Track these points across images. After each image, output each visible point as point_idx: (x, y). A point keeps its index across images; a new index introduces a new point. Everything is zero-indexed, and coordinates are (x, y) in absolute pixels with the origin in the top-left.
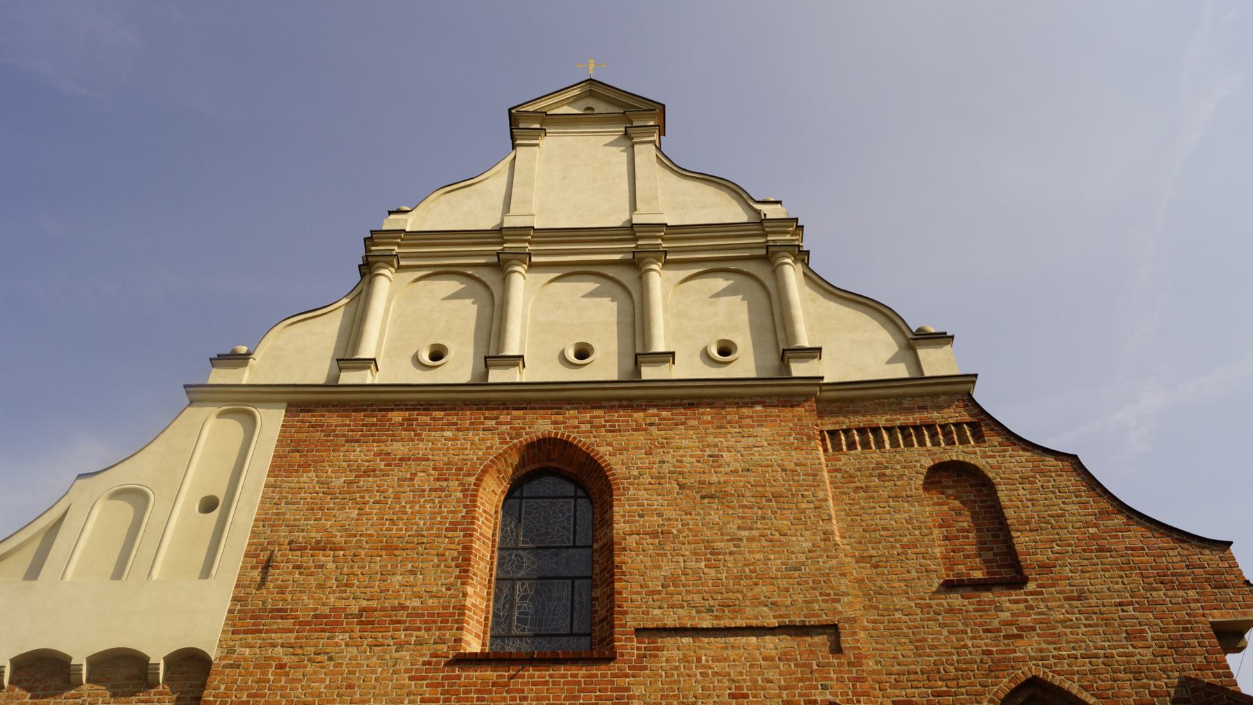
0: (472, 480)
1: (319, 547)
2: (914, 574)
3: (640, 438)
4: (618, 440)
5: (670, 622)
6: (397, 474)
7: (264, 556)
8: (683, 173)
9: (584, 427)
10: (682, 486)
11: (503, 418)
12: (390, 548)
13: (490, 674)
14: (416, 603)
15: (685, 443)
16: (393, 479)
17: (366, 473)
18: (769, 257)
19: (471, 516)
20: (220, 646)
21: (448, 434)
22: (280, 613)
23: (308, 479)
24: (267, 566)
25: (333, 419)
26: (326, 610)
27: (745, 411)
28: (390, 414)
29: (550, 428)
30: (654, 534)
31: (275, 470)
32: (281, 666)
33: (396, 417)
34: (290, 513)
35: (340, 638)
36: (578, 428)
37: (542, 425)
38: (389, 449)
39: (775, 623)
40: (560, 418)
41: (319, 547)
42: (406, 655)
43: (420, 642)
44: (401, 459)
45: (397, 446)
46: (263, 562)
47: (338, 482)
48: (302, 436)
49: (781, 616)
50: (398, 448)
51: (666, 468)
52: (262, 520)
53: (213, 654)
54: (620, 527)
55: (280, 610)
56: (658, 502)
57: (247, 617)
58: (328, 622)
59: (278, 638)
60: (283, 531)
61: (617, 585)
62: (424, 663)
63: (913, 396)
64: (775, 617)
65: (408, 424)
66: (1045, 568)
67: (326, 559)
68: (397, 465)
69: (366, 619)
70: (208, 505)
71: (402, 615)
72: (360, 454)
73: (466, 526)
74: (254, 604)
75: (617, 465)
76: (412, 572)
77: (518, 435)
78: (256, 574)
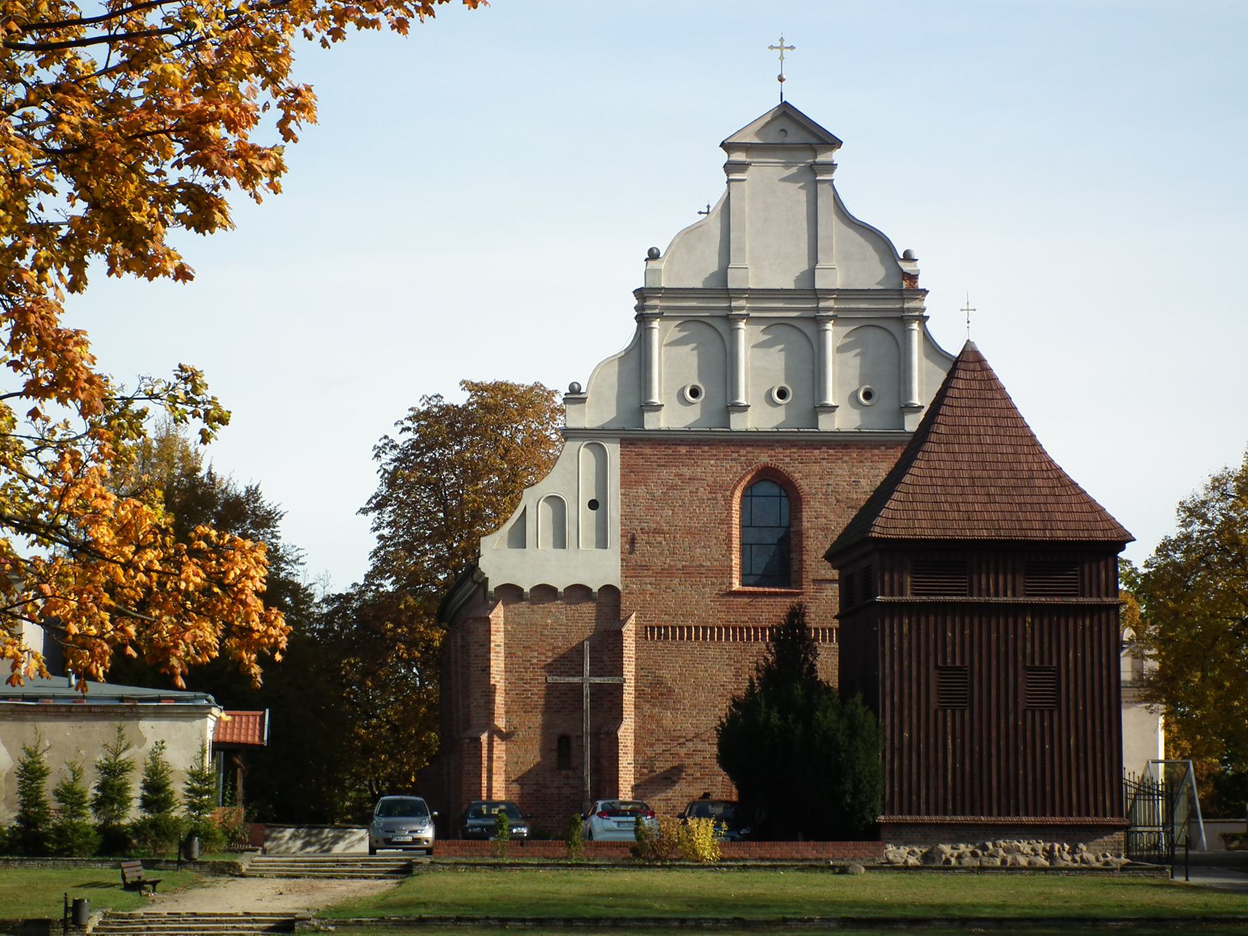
0: (728, 493)
1: (658, 531)
3: (816, 468)
9: (787, 460)
10: (838, 501)
11: (743, 452)
13: (746, 600)
15: (840, 472)
17: (673, 487)
18: (903, 320)
19: (730, 516)
21: (712, 462)
23: (641, 490)
24: (632, 541)
25: (648, 451)
27: (876, 451)
28: (679, 448)
29: (768, 459)
31: (625, 483)
33: (683, 450)
34: (639, 512)
35: (676, 581)
36: (786, 461)
37: (764, 458)
38: (681, 472)
40: (773, 453)
41: (658, 531)
42: (707, 590)
43: (713, 584)
48: (632, 462)
50: (686, 472)
52: (626, 517)
54: (806, 524)
57: (630, 568)
58: (668, 572)
59: (647, 580)
61: (805, 557)
65: (689, 455)
69: (686, 572)
73: (728, 521)
75: (804, 485)
77: (751, 464)
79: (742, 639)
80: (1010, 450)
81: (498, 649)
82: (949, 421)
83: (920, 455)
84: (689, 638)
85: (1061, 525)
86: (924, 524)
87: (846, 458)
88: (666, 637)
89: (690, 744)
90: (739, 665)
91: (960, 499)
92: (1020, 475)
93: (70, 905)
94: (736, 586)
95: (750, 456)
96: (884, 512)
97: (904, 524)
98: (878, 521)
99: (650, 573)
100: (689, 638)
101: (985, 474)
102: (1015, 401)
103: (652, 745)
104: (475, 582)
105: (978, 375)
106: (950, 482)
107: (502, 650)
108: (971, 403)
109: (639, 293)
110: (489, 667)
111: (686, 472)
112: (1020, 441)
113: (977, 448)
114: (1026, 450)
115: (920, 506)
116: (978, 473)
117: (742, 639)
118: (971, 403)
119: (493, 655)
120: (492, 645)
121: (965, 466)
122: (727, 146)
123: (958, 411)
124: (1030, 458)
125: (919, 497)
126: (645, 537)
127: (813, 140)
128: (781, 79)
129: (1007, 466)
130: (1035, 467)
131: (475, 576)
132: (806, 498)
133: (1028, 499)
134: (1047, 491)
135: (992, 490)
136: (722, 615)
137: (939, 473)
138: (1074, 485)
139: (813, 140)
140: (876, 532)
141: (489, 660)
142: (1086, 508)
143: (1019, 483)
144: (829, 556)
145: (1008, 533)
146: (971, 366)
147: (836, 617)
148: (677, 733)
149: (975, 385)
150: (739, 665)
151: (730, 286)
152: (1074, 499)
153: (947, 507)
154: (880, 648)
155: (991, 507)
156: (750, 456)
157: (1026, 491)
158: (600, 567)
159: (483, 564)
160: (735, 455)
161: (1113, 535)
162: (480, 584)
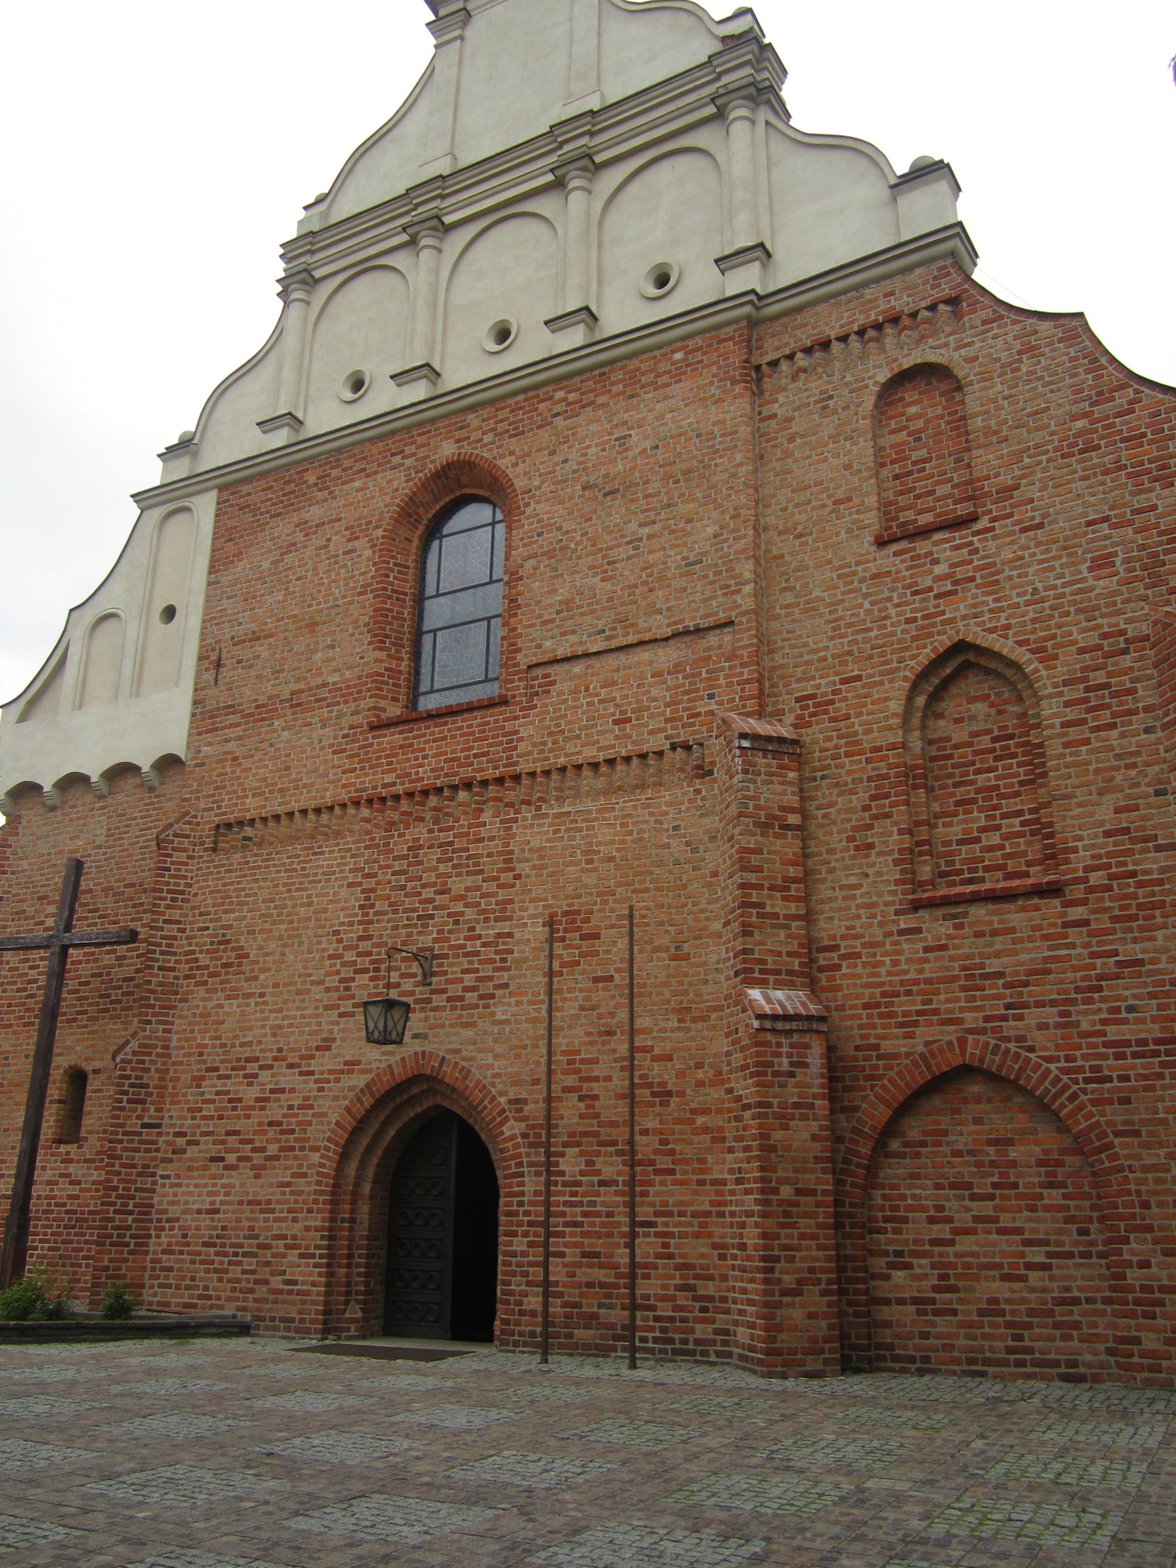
2: (843, 535)
3: (545, 435)
5: (560, 653)
6: (316, 541)
7: (214, 657)
14: (335, 678)
15: (593, 428)
20: (188, 747)
21: (357, 484)
22: (230, 709)
24: (218, 665)
26: (263, 700)
30: (550, 554)
32: (235, 759)
37: (447, 450)
39: (669, 631)
44: (317, 526)
46: (212, 661)
47: (266, 565)
49: (676, 623)
50: (315, 513)
55: (229, 707)
57: (205, 718)
59: (232, 733)
62: (344, 736)
63: (878, 280)
64: (668, 626)
66: (1006, 492)
67: (262, 649)
68: (315, 533)
69: (296, 703)
71: (324, 693)
72: (283, 529)
74: (210, 705)
76: (332, 647)
77: (424, 467)
78: (209, 676)
89: (264, 1076)
90: (370, 883)
99: (236, 718)
103: (198, 1080)
126: (237, 651)
136: (351, 778)
150: (370, 883)
160: (397, 459)
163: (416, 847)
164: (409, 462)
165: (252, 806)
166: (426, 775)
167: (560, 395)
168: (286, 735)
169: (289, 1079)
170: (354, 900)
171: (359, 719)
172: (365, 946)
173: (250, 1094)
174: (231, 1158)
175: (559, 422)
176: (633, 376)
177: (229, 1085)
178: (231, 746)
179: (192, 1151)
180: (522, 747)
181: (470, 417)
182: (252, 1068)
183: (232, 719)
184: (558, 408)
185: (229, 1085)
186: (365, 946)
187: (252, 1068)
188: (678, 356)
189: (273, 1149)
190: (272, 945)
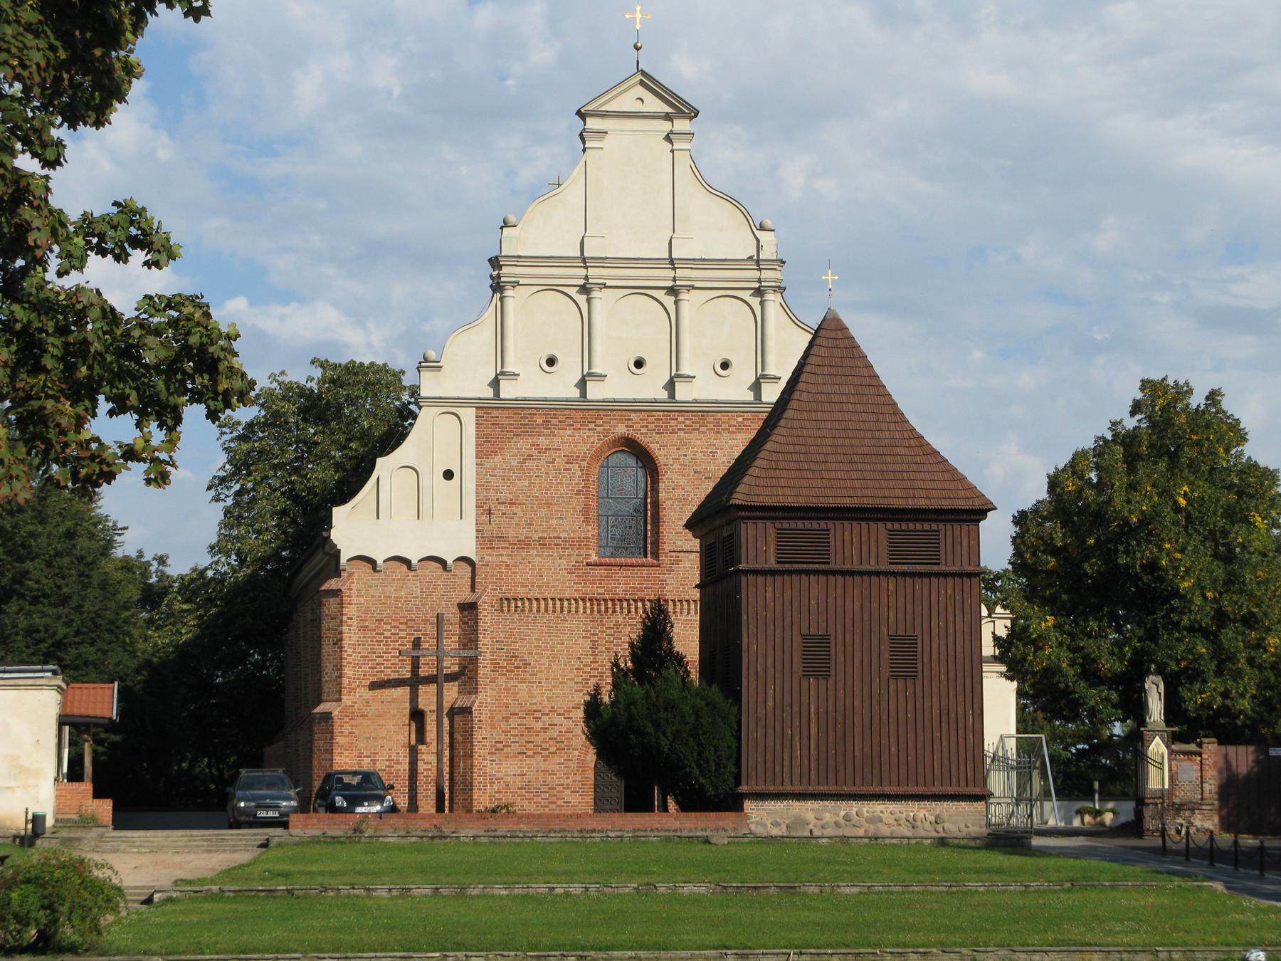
0: (585, 464)
1: (512, 503)
3: (674, 438)
4: (665, 439)
5: (685, 548)
8: (710, 188)
9: (644, 430)
12: (548, 505)
14: (565, 535)
15: (698, 442)
16: (543, 462)
21: (569, 432)
30: (679, 500)
31: (479, 455)
37: (621, 430)
41: (512, 503)
42: (564, 561)
45: (542, 439)
46: (485, 510)
47: (515, 463)
50: (543, 441)
51: (688, 459)
53: (474, 557)
56: (682, 481)
57: (485, 541)
58: (524, 544)
59: (505, 552)
60: (492, 493)
69: (542, 543)
70: (448, 475)
72: (523, 444)
75: (661, 456)
79: (599, 612)
80: (872, 418)
81: (350, 622)
82: (812, 388)
83: (782, 423)
84: (546, 610)
85: (923, 493)
86: (787, 491)
87: (702, 429)
88: (523, 611)
91: (823, 467)
92: (883, 443)
93: (30, 817)
94: (594, 558)
95: (607, 426)
96: (746, 479)
97: (767, 491)
98: (741, 488)
99: (506, 545)
100: (546, 610)
101: (847, 442)
102: (877, 369)
103: (507, 719)
104: (327, 554)
105: (841, 343)
106: (813, 450)
107: (354, 623)
108: (833, 371)
109: (495, 262)
110: (341, 640)
111: (543, 441)
112: (883, 409)
113: (839, 416)
114: (888, 418)
115: (784, 474)
116: (841, 441)
117: (599, 612)
118: (833, 371)
119: (345, 629)
120: (345, 618)
121: (827, 434)
122: (582, 115)
123: (820, 379)
124: (892, 427)
125: (782, 465)
126: (502, 508)
127: (670, 110)
128: (637, 49)
129: (870, 434)
130: (897, 435)
131: (327, 549)
132: (662, 469)
133: (891, 467)
134: (910, 459)
135: (855, 458)
137: (802, 440)
138: (936, 453)
139: (670, 110)
140: (738, 498)
141: (341, 633)
142: (948, 476)
143: (881, 451)
144: (690, 525)
145: (871, 501)
146: (833, 334)
147: (697, 586)
148: (535, 707)
149: (837, 352)
151: (586, 255)
152: (935, 468)
153: (809, 474)
154: (744, 617)
155: (854, 475)
156: (607, 426)
157: (889, 459)
158: (455, 536)
159: (337, 535)
161: (976, 504)
162: (332, 556)
163: (617, 625)
164: (599, 429)
165: (521, 592)
166: (620, 592)
167: (681, 419)
168: (538, 559)
169: (557, 720)
170: (587, 644)
171: (581, 559)
172: (593, 665)
173: (539, 725)
174: (530, 753)
175: (681, 433)
176: (718, 425)
177: (524, 721)
178: (505, 558)
179: (506, 750)
180: (668, 588)
181: (633, 415)
182: (537, 715)
183: (503, 544)
184: (683, 426)
185: (524, 721)
186: (593, 665)
187: (537, 715)
188: (740, 419)
189: (553, 749)
190: (543, 661)
